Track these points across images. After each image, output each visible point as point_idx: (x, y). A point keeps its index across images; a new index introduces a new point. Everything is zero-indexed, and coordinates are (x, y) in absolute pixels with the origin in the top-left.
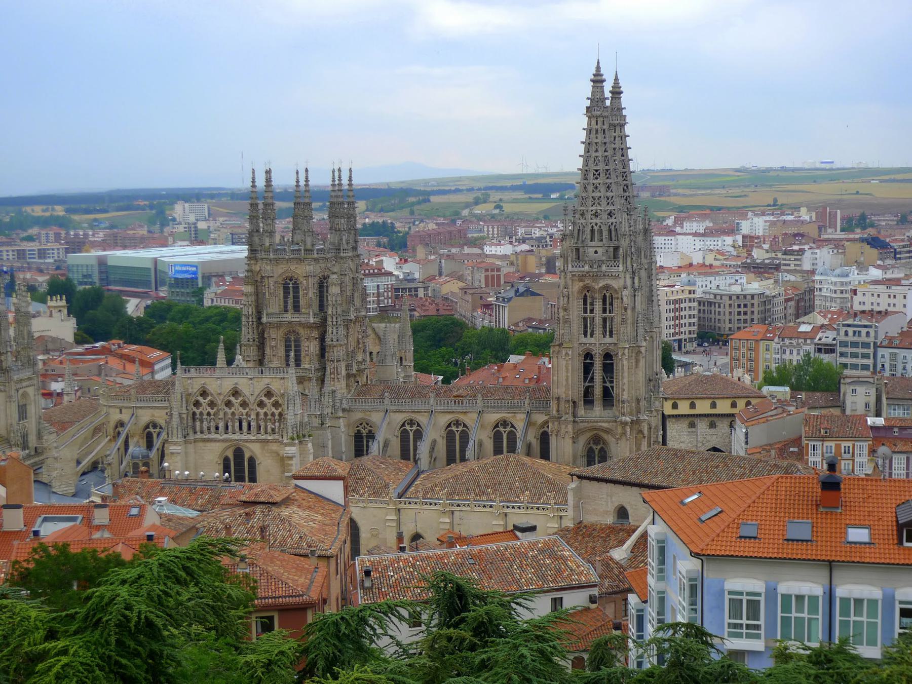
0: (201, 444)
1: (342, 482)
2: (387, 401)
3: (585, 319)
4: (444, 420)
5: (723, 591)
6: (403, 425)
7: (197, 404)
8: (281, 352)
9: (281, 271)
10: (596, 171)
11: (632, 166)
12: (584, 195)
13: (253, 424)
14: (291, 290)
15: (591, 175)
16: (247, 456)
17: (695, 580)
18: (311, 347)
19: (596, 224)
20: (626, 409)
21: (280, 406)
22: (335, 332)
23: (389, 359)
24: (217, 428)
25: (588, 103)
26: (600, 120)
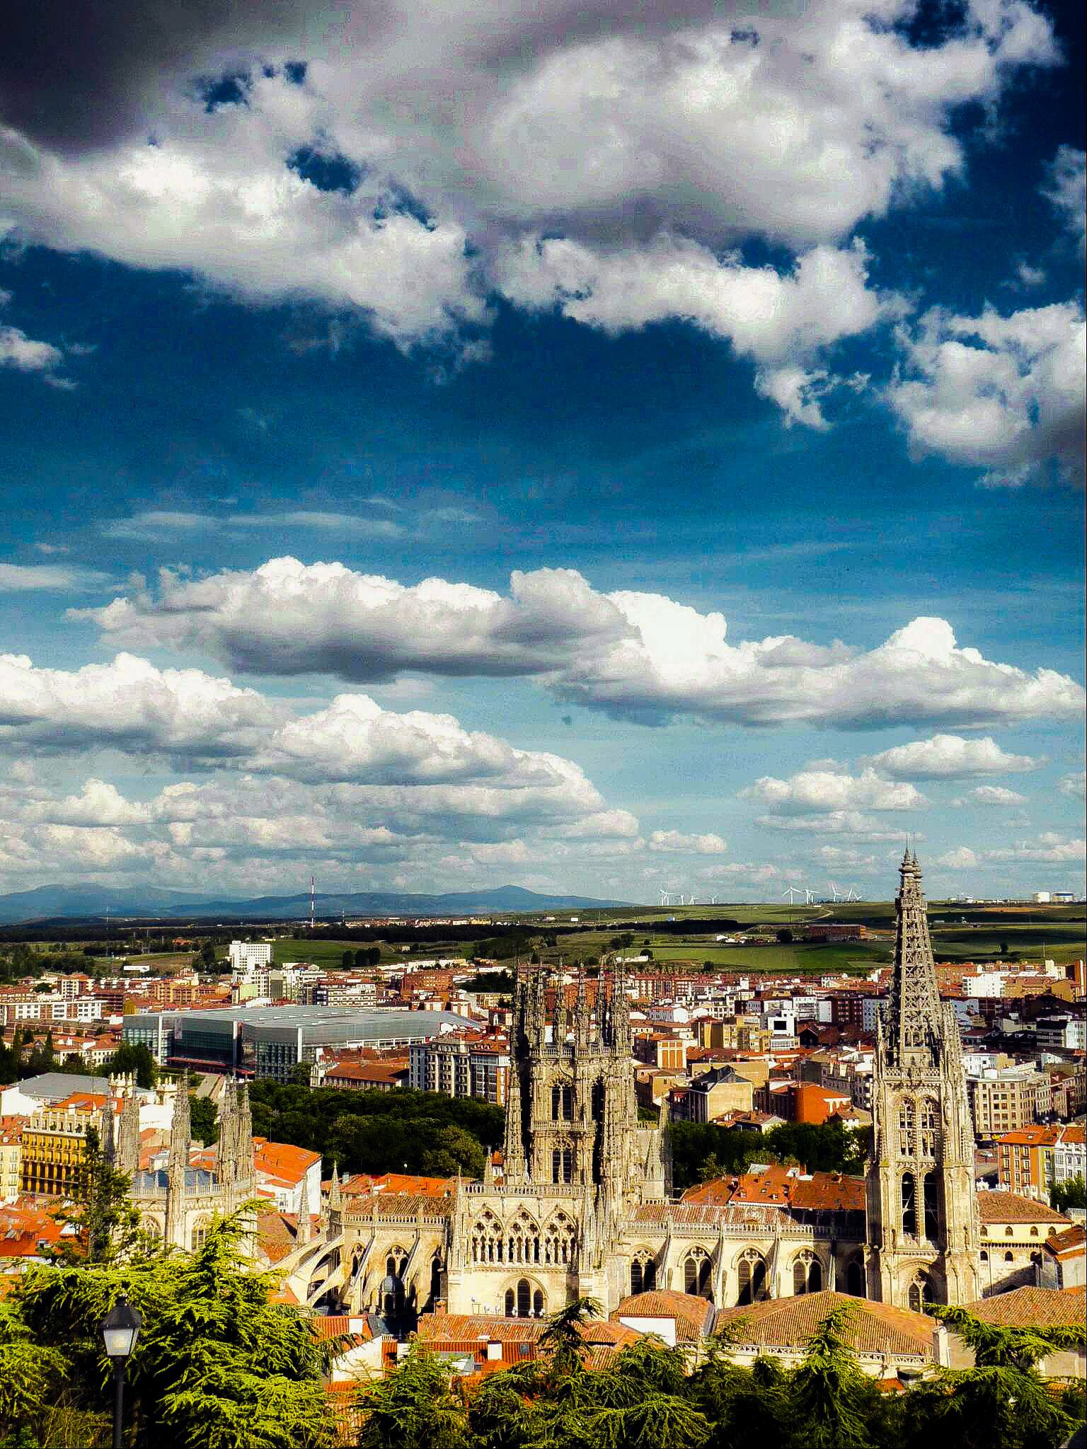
10: (909, 968)
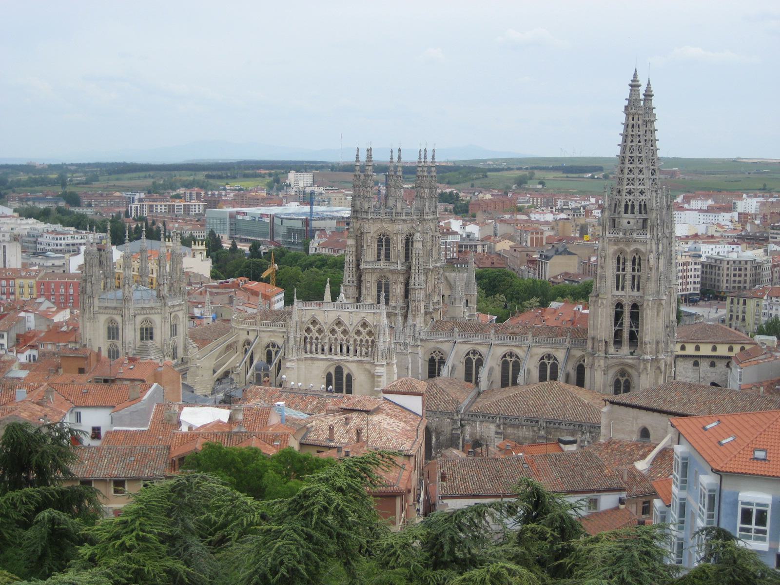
0: (310, 362)
1: (420, 398)
2: (456, 334)
3: (618, 276)
4: (500, 351)
5: (735, 503)
6: (468, 354)
7: (308, 330)
8: (374, 291)
9: (376, 229)
10: (631, 157)
11: (660, 154)
12: (621, 176)
13: (351, 348)
14: (384, 243)
15: (627, 160)
16: (345, 373)
17: (714, 491)
18: (398, 289)
19: (630, 200)
20: (648, 349)
21: (373, 334)
22: (417, 279)
23: (457, 301)
24: (323, 350)
25: (626, 103)
26: (636, 117)
